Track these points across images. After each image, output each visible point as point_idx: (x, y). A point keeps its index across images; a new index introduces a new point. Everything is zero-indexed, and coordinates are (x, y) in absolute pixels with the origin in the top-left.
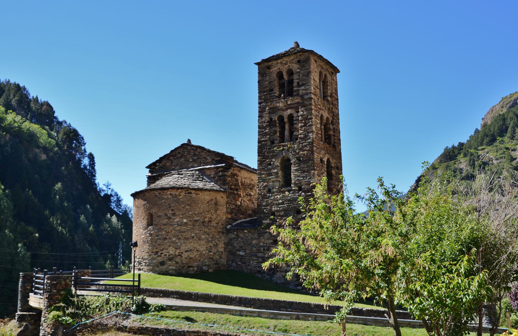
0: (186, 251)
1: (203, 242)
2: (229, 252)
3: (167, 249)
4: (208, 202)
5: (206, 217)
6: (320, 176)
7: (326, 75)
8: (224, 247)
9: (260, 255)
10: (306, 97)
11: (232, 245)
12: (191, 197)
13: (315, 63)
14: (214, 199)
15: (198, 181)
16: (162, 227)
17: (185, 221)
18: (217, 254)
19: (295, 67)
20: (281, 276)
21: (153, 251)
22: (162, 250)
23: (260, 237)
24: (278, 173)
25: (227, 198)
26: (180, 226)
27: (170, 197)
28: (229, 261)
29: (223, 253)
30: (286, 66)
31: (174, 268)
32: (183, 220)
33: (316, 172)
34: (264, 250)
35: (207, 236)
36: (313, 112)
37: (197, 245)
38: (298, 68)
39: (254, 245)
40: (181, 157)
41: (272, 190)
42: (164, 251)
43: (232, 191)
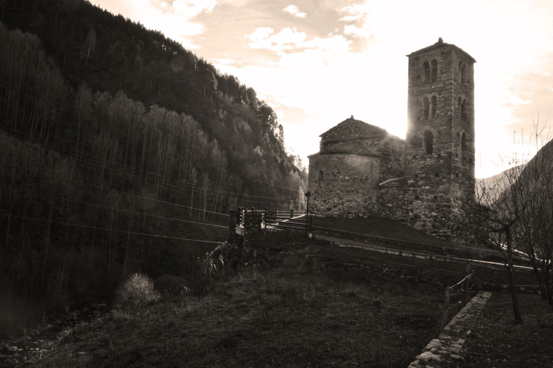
0: (347, 201)
1: (360, 195)
2: (380, 203)
3: (333, 199)
4: (365, 164)
5: (363, 176)
6: (456, 147)
7: (464, 65)
8: (376, 200)
9: (404, 207)
10: (447, 82)
11: (383, 199)
12: (352, 160)
13: (456, 55)
14: (370, 162)
15: (358, 148)
16: (330, 182)
17: (347, 178)
18: (371, 205)
19: (439, 59)
20: (420, 225)
21: (323, 200)
22: (329, 200)
23: (405, 193)
24: (422, 144)
25: (381, 162)
27: (336, 159)
28: (380, 210)
29: (376, 204)
30: (432, 58)
31: (337, 213)
32: (345, 178)
33: (453, 144)
34: (408, 203)
35: (364, 191)
36: (453, 95)
38: (442, 59)
39: (400, 199)
40: (346, 129)
41: (416, 157)
42: (330, 200)
43: (384, 156)
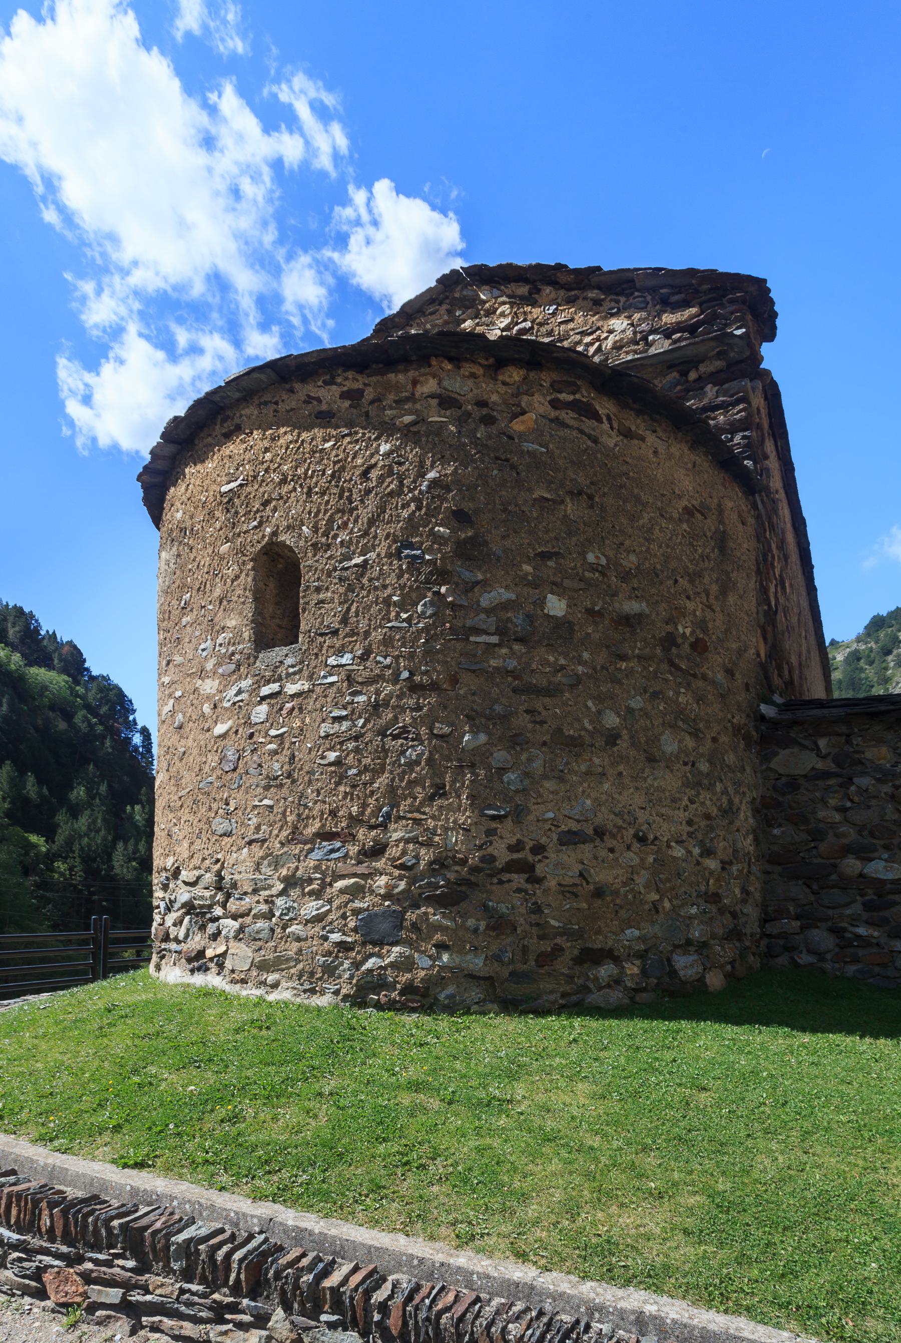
0: (570, 839)
26: (521, 640)
32: (541, 603)
37: (639, 800)
